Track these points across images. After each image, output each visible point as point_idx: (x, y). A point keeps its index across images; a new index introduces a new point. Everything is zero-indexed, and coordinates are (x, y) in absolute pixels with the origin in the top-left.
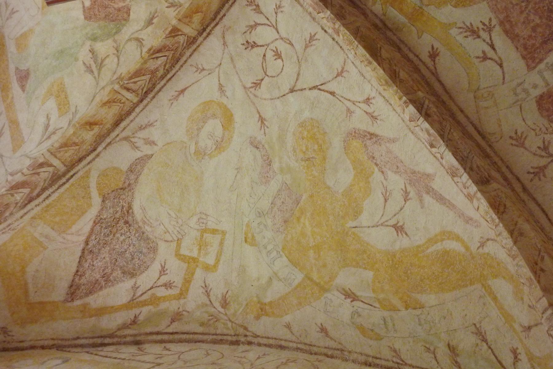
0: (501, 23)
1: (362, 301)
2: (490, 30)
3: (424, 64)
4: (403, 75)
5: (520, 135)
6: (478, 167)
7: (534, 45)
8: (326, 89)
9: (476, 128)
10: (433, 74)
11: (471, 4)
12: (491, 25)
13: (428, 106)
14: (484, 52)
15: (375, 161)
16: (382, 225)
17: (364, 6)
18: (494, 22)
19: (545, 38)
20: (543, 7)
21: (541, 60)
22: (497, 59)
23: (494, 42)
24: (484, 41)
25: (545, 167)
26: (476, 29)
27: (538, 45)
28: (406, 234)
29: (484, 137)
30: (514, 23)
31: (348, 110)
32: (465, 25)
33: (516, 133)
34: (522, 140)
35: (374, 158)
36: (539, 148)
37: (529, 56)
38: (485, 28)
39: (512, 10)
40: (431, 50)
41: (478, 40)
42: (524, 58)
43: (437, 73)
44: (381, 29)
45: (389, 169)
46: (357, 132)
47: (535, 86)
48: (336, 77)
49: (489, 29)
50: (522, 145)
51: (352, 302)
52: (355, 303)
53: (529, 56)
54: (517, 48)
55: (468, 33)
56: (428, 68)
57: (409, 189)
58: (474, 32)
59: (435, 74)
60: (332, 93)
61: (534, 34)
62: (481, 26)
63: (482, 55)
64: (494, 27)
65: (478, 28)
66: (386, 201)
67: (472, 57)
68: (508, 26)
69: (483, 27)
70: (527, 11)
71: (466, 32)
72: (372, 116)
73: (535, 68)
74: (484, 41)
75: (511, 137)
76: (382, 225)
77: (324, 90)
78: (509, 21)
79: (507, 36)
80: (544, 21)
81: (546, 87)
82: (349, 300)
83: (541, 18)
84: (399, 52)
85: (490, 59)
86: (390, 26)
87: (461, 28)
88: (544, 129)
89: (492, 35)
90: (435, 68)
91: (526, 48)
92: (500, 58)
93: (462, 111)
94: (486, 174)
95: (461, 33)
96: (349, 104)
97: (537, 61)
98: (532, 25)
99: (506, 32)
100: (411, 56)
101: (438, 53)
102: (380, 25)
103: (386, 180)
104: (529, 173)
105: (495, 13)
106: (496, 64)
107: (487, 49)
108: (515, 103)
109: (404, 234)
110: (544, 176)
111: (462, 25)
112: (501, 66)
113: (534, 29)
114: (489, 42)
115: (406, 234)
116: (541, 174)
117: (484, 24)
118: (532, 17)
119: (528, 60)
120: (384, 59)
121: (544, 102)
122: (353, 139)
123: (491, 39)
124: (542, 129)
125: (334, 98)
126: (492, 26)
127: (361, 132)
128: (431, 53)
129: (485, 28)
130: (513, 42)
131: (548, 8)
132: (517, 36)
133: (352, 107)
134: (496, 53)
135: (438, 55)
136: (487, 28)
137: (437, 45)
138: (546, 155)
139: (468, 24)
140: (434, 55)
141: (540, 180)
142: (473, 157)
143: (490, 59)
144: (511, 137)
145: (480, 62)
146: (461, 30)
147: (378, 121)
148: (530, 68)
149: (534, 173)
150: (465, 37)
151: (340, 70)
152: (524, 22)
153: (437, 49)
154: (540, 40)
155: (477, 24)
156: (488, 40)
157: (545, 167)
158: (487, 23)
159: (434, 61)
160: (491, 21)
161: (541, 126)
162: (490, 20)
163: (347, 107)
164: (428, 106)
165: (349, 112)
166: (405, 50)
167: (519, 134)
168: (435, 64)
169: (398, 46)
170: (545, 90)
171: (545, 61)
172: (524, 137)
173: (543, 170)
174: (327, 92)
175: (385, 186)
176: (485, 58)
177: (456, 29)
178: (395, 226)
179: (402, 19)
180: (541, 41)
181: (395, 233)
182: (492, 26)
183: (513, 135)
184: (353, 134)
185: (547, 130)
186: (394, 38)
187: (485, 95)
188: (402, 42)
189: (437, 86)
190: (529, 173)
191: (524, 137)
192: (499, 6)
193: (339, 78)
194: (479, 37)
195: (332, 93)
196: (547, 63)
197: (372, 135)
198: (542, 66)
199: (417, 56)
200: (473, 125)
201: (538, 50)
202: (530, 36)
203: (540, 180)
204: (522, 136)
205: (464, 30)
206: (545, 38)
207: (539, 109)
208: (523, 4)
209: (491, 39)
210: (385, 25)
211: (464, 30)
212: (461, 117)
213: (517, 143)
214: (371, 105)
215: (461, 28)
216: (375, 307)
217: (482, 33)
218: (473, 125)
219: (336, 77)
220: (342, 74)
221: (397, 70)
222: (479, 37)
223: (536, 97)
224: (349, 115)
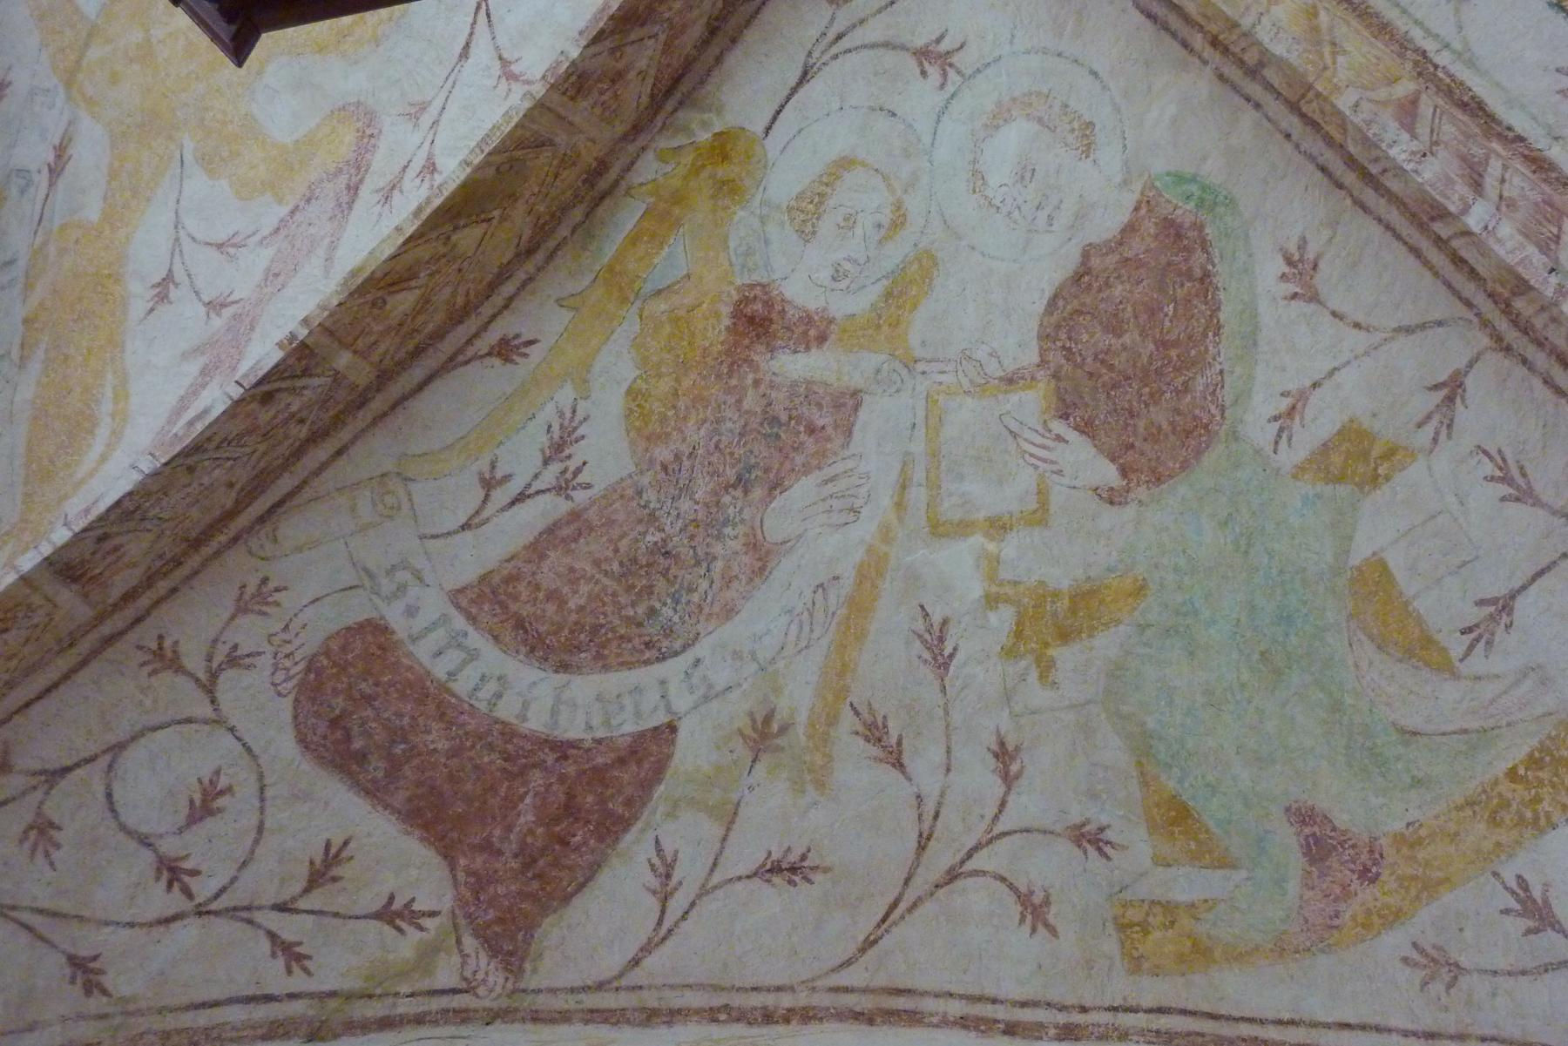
0: (575, 516)
1: (47, 196)
2: (561, 488)
3: (485, 327)
4: (403, 302)
5: (270, 599)
6: (116, 549)
7: (516, 598)
8: (478, 28)
9: (291, 495)
10: (451, 359)
11: (632, 434)
12: (574, 488)
13: (304, 388)
14: (507, 478)
15: (302, 204)
16: (177, 239)
17: (659, 124)
18: (580, 496)
19: (531, 624)
20: (604, 613)
21: (472, 619)
22: (485, 514)
23: (529, 502)
24: (536, 476)
25: (180, 669)
26: (567, 452)
27: (513, 607)
28: (152, 310)
29: (262, 519)
30: (573, 546)
31: (423, 107)
32: (581, 423)
33: (277, 590)
34: (257, 607)
35: (308, 201)
36: (235, 647)
37: (487, 590)
38: (569, 475)
39: (605, 539)
40: (524, 339)
41: (539, 461)
42: (483, 579)
43: (455, 367)
44: (592, 186)
45: (279, 251)
46: (373, 141)
47: (411, 612)
48: (501, 58)
49: (562, 488)
50: (241, 609)
51: (49, 165)
52: (46, 170)
53: (487, 590)
54: (508, 561)
55: (556, 435)
56: (469, 342)
57: (228, 312)
58: (557, 449)
59: (450, 364)
60: (465, 52)
61: (541, 595)
62: (572, 465)
63: (499, 474)
64: (568, 497)
65: (569, 457)
66: (220, 246)
67: (497, 452)
68: (566, 532)
69: (572, 469)
70: (597, 576)
71: (562, 426)
72: (393, 187)
73: (458, 606)
74: (536, 476)
75: (265, 581)
76: (177, 239)
77: (474, 22)
78: (580, 534)
79: (541, 534)
80: (574, 617)
81: (410, 636)
82: (51, 158)
83: (581, 609)
84: (518, 255)
85: (487, 496)
86: (600, 210)
87: (574, 412)
88: (288, 649)
89: (548, 494)
90: (467, 362)
91: (511, 579)
92: (487, 520)
93: (339, 453)
94: (97, 571)
95: (561, 415)
96: (434, 110)
97: (474, 610)
98: (566, 590)
99: (551, 530)
100: (508, 288)
101: (512, 361)
102: (603, 184)
103: (261, 242)
104: (161, 637)
105: (604, 497)
106: (473, 512)
107: (514, 488)
108: (366, 570)
109: (151, 304)
110: (154, 672)
111: (580, 415)
112: (465, 527)
113: (552, 595)
114: (532, 491)
115: (152, 310)
116: (158, 665)
117: (578, 471)
118: (584, 588)
119: (476, 590)
120: (448, 238)
121: (370, 638)
122: (358, 131)
123: (538, 492)
124: (288, 646)
125: (455, 60)
126: (573, 494)
127: (368, 156)
128: (516, 342)
129: (569, 475)
130: (526, 548)
131: (602, 626)
132: (543, 557)
133: (426, 120)
134: (503, 510)
135: (507, 360)
136: (567, 482)
137: (535, 353)
138: (215, 665)
139: (580, 432)
140: (506, 350)
141: (144, 664)
142: (149, 531)
143: (487, 496)
144: (265, 581)
145: (481, 474)
146: (568, 415)
147: (379, 206)
148: (456, 596)
149: (161, 648)
150: (550, 427)
151: (515, 68)
152: (572, 570)
153: (526, 355)
154: (526, 611)
155: (579, 452)
156: (537, 486)
157: (180, 669)
158: (581, 479)
159: (489, 354)
160: (585, 488)
161: (297, 642)
162: (588, 486)
163: (430, 103)
164: (304, 388)
165: (416, 112)
166: (530, 267)
167: (277, 596)
168: (482, 357)
169: (538, 247)
170: (401, 634)
171: (470, 630)
172: (265, 608)
173: (170, 667)
174: (471, 34)
175: (248, 241)
176: (489, 484)
177: (571, 400)
178: (169, 278)
179: (610, 250)
180: (525, 614)
181: (158, 279)
182: (573, 494)
183: (271, 585)
184: (368, 132)
185: (287, 656)
186: (564, 231)
187: (389, 500)
188: (551, 256)
189: (417, 373)
190: (161, 637)
191: (265, 608)
192: (617, 505)
193: (496, 68)
194: (546, 462)
195: (465, 52)
196: (466, 634)
197: (354, 189)
198: (460, 622)
199: (506, 307)
200: (298, 489)
201: (499, 611)
202: (538, 587)
203: (144, 664)
204: (267, 604)
205: (566, 423)
206: (531, 624)
207: (349, 629)
208: (616, 566)
209: (538, 492)
210: (602, 198)
211: (566, 423)
212: (321, 453)
213: (247, 597)
214: (418, 181)
215: (574, 412)
216: (35, 233)
217: (555, 468)
218: (298, 489)
219: (501, 58)
220: (503, 80)
221: (413, 283)
222: (546, 462)
223: (382, 618)
224: (413, 111)
